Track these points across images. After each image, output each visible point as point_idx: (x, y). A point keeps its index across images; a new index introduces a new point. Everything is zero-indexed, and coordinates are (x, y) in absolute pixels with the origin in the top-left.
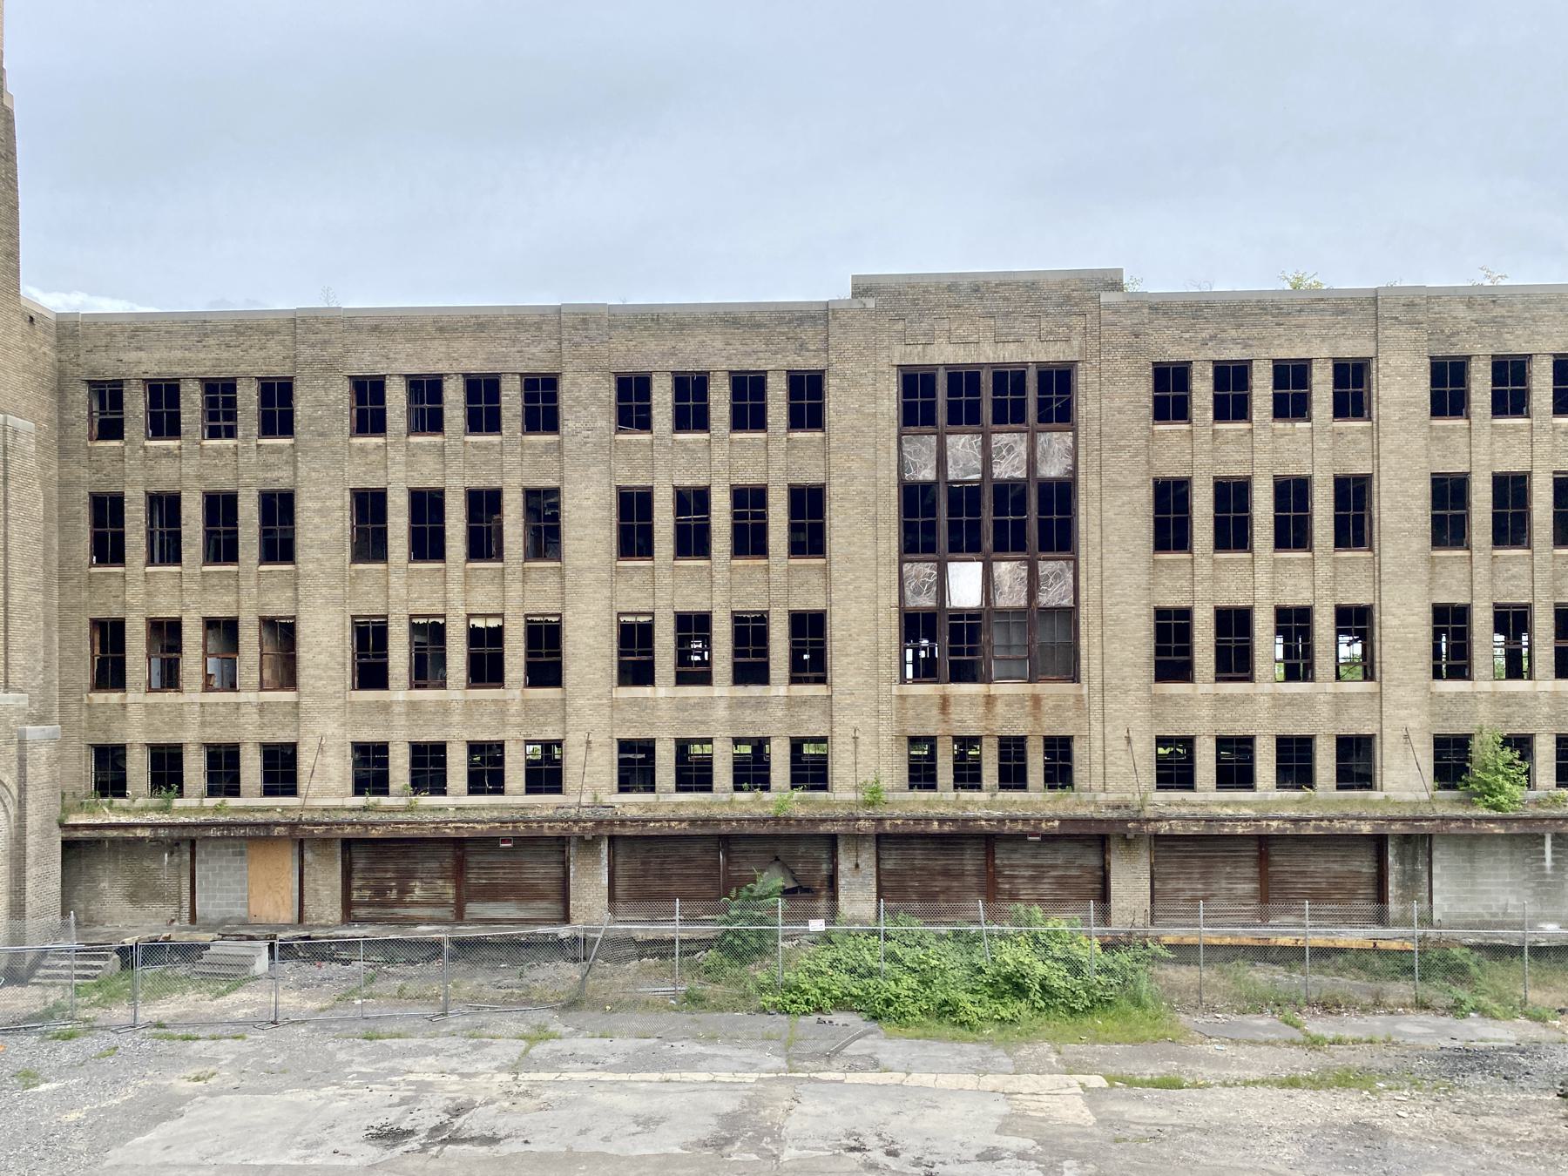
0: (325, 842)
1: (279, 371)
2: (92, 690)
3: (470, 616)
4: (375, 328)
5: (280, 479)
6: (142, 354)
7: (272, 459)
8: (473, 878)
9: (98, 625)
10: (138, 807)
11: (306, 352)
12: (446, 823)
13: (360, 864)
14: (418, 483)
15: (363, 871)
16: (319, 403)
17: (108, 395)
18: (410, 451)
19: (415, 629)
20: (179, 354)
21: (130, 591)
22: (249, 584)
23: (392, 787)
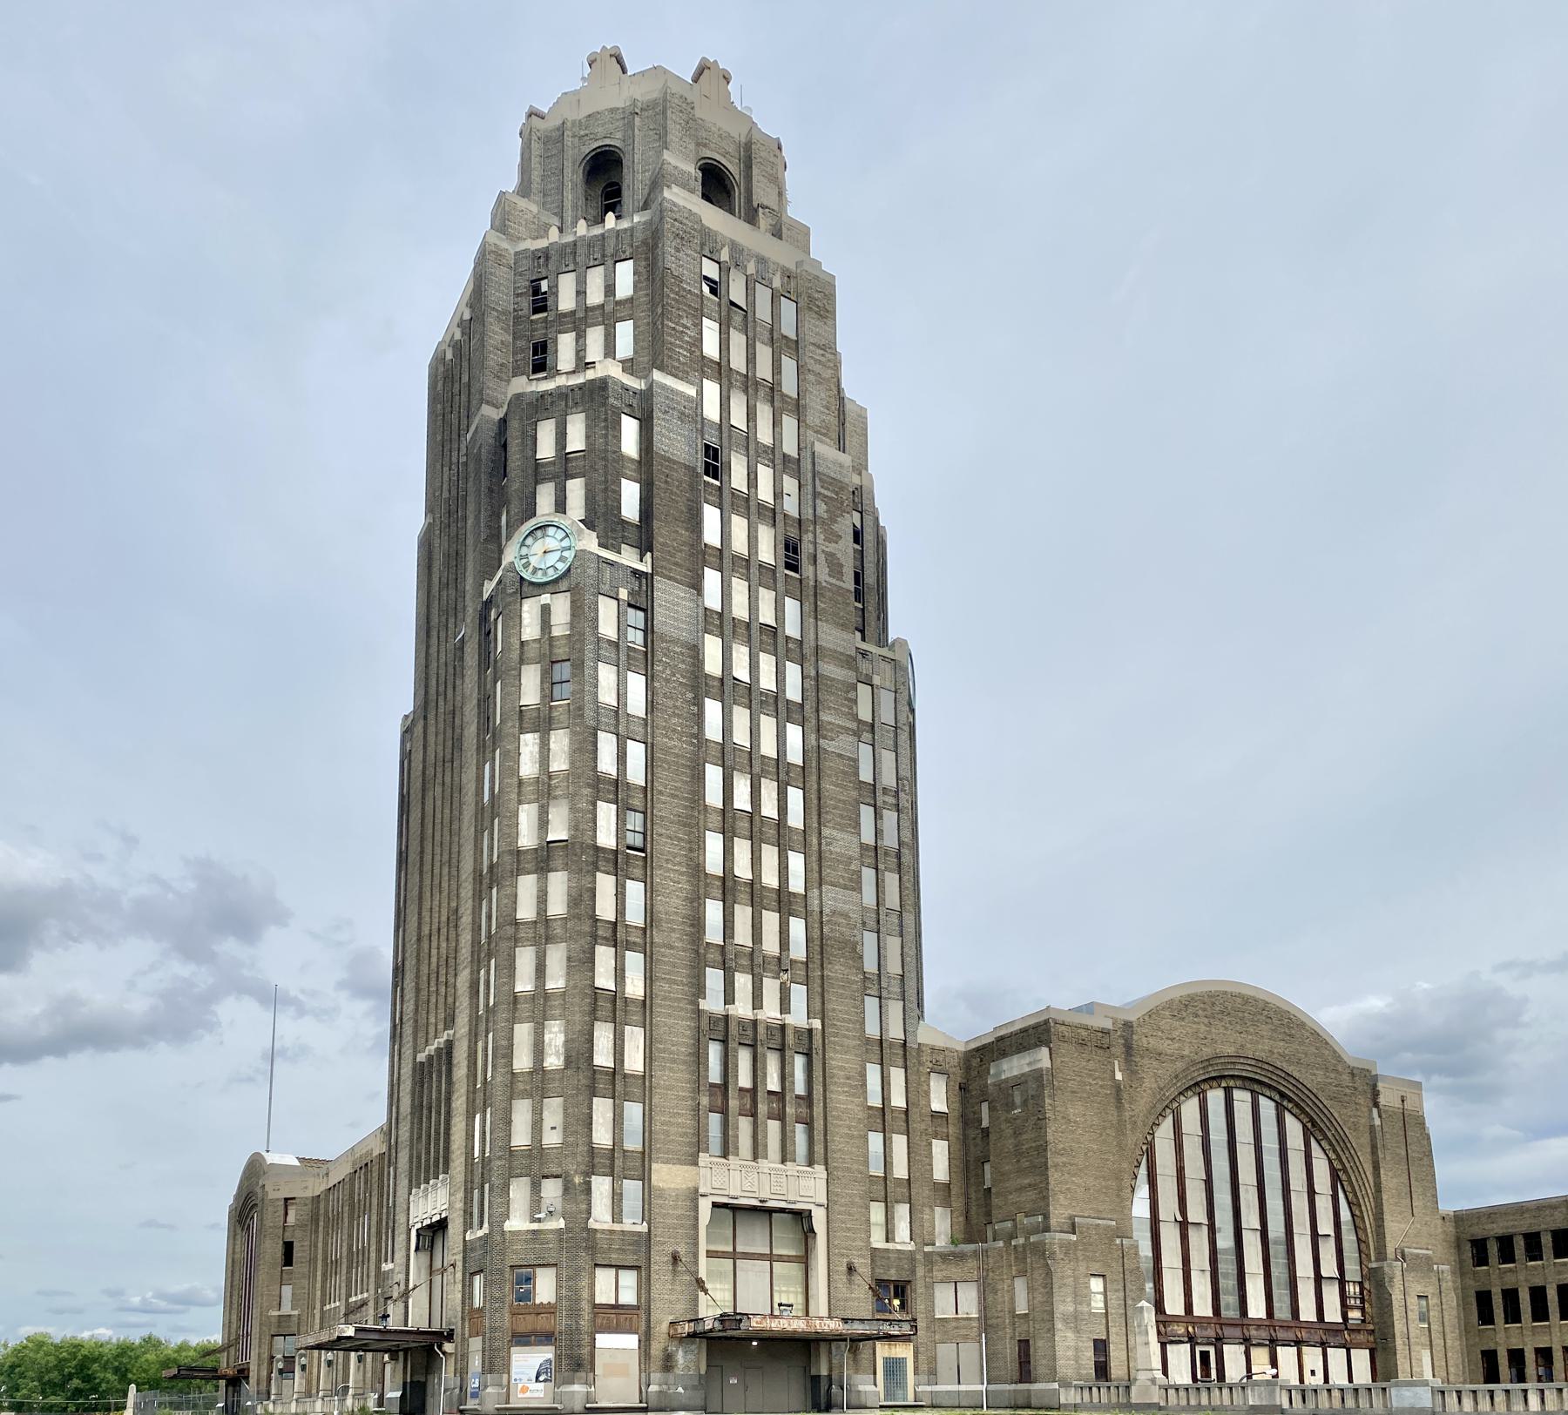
9: (1484, 1353)
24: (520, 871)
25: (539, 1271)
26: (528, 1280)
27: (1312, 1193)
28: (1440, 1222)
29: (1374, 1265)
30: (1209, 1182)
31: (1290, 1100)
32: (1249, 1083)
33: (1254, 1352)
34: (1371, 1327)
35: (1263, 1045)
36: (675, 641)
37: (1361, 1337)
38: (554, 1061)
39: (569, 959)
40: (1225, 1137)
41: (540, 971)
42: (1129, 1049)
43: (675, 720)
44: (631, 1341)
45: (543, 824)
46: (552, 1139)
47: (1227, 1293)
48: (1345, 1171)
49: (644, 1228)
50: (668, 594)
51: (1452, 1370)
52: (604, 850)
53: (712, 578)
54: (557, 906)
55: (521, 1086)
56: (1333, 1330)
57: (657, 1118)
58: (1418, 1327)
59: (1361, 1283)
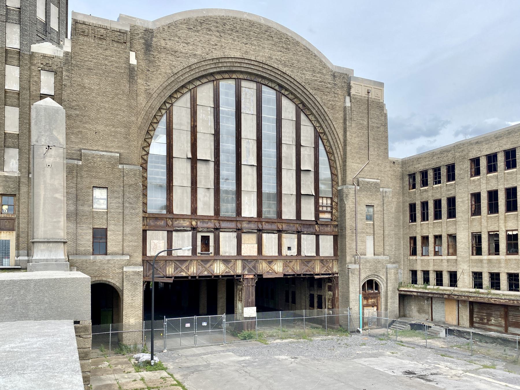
0: (465, 301)
1: (451, 162)
2: (410, 255)
3: (507, 231)
4: (477, 143)
5: (451, 194)
6: (419, 165)
7: (450, 188)
8: (510, 319)
9: (411, 238)
10: (419, 287)
11: (458, 155)
12: (492, 298)
13: (476, 310)
14: (490, 189)
15: (477, 312)
16: (461, 169)
17: (412, 176)
18: (488, 179)
19: (490, 235)
20: (427, 163)
21: (418, 229)
22: (444, 225)
23: (484, 286)
27: (298, 146)
28: (388, 165)
29: (339, 188)
30: (217, 135)
31: (287, 90)
32: (252, 77)
33: (244, 237)
34: (336, 223)
35: (262, 53)
37: (328, 229)
40: (233, 109)
42: (148, 47)
47: (228, 202)
48: (325, 133)
51: (387, 248)
56: (308, 224)
58: (362, 224)
59: (331, 198)
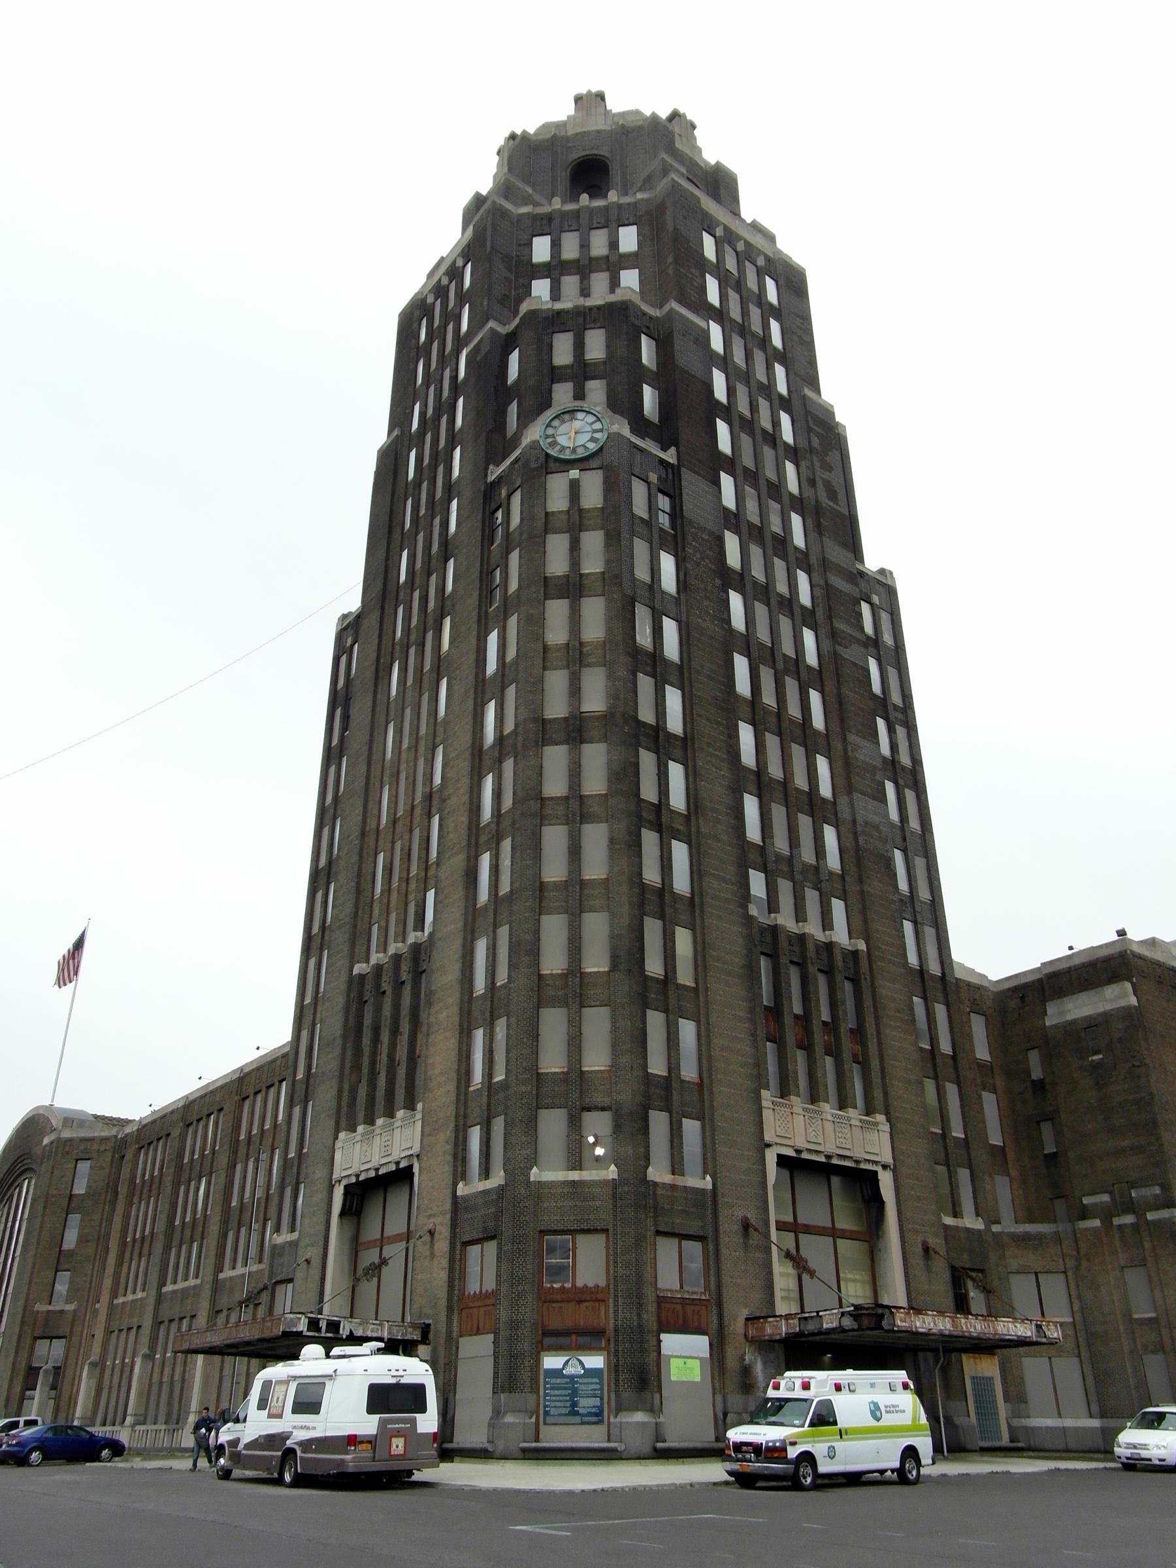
24: (545, 741)
25: (580, 1238)
26: (569, 1252)
36: (704, 529)
38: (596, 963)
39: (612, 841)
41: (575, 852)
43: (706, 603)
44: (700, 1344)
45: (575, 691)
46: (596, 1060)
49: (707, 1183)
50: (691, 483)
52: (644, 724)
53: (727, 482)
54: (595, 783)
55: (551, 992)
57: (718, 1042)
